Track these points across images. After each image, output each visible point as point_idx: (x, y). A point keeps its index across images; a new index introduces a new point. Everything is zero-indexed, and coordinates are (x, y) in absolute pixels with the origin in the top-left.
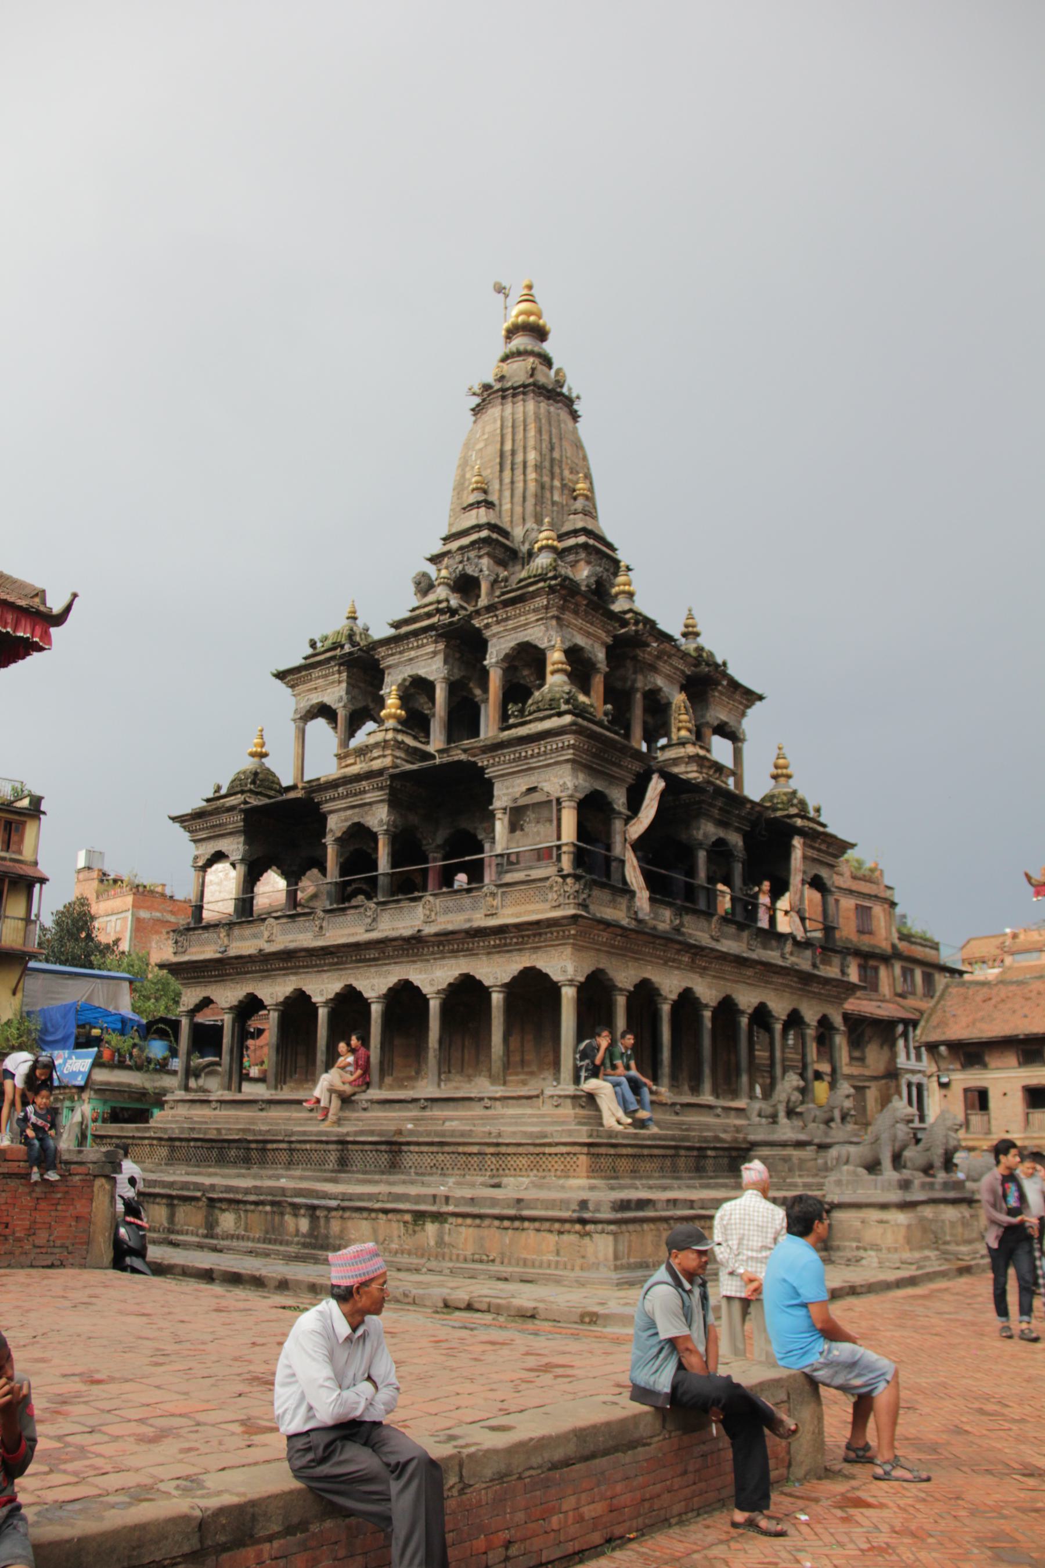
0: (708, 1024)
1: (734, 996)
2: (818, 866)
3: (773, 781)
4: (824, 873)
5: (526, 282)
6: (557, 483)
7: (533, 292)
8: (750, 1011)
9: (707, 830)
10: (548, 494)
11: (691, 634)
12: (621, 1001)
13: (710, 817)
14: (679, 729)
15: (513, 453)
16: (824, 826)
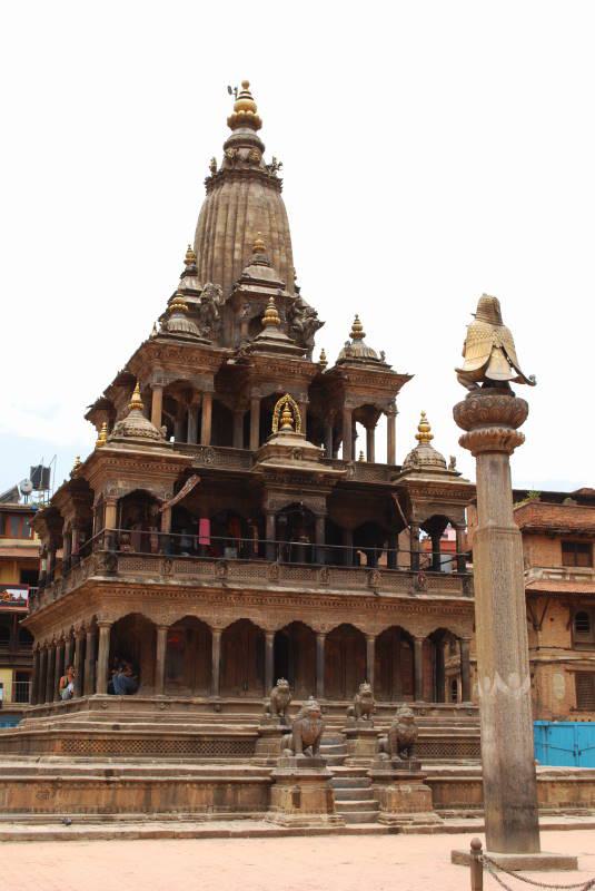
0: (271, 645)
1: (305, 621)
2: (439, 508)
3: (417, 442)
4: (449, 513)
5: (245, 79)
6: (238, 245)
7: (250, 89)
9: (276, 500)
10: (229, 256)
11: (357, 334)
12: (162, 634)
13: (279, 491)
14: (280, 425)
15: (210, 228)
16: (458, 474)
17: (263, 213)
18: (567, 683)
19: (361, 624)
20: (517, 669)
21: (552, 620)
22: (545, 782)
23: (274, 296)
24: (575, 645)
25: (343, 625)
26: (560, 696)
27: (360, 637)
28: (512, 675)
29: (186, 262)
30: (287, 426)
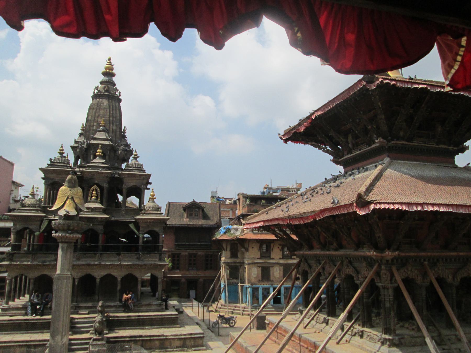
6: (95, 124)
8: (100, 277)
10: (92, 128)
14: (92, 197)
17: (107, 111)
18: (258, 271)
19: (115, 274)
20: (60, 334)
21: (253, 248)
22: (170, 339)
23: (102, 144)
24: (262, 257)
25: (107, 274)
26: (255, 276)
27: (115, 278)
28: (58, 337)
29: (81, 130)
30: (93, 198)
